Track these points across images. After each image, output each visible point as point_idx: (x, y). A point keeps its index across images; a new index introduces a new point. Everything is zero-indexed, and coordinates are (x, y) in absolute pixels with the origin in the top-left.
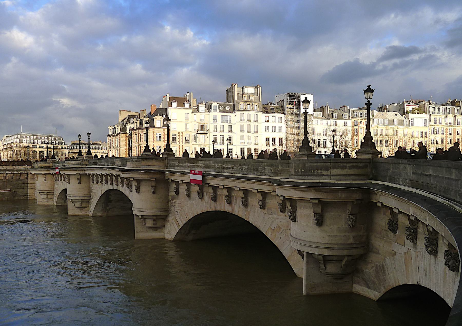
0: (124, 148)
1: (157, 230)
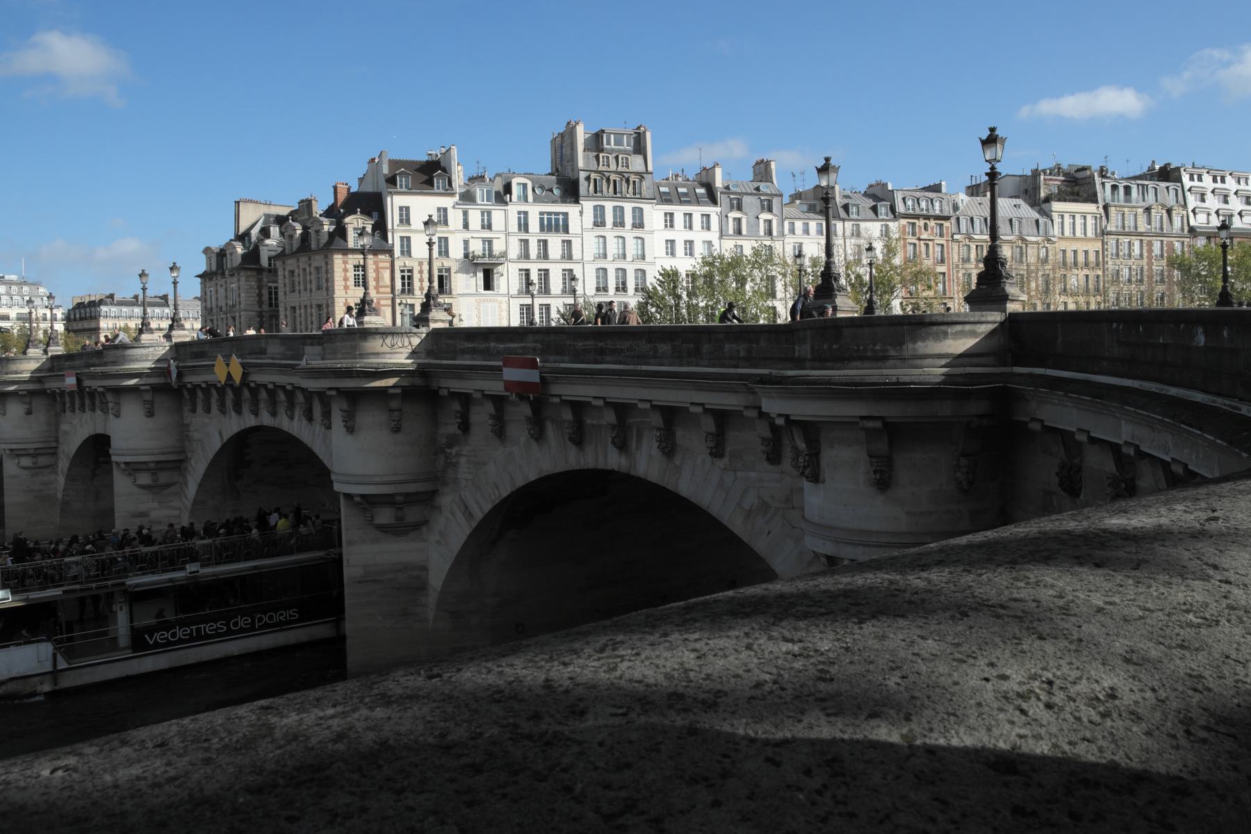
0: (254, 313)
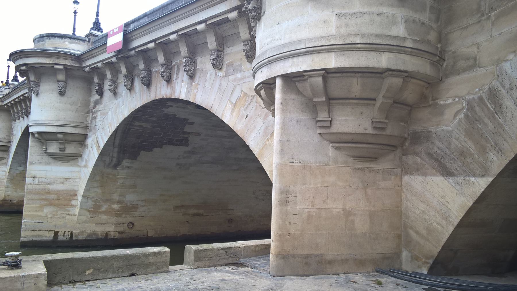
1: (68, 161)
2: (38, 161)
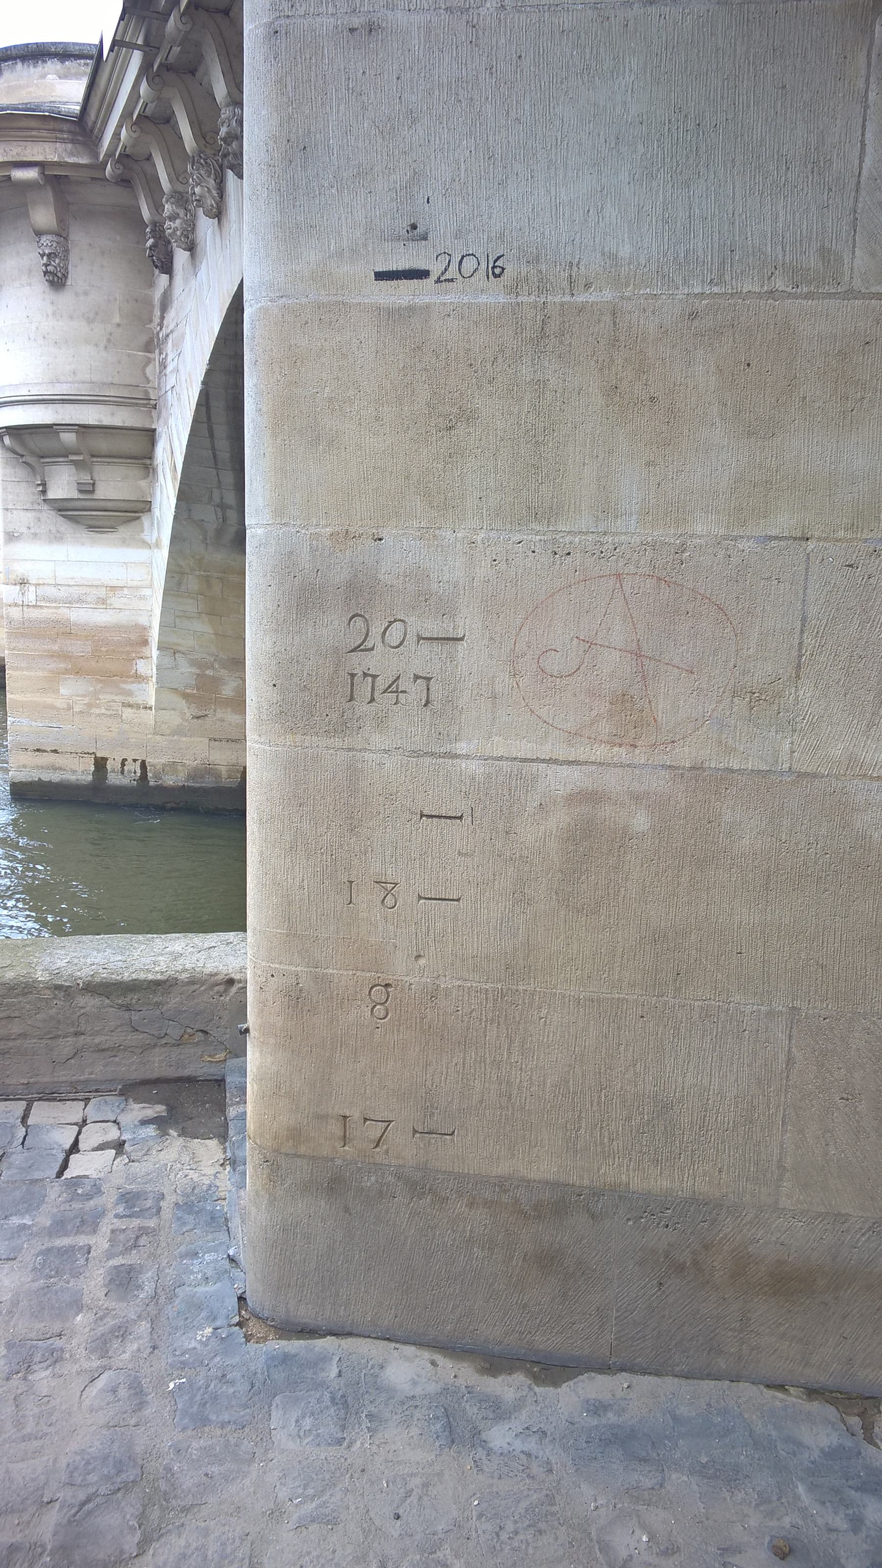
1: (113, 528)
2: (29, 528)
